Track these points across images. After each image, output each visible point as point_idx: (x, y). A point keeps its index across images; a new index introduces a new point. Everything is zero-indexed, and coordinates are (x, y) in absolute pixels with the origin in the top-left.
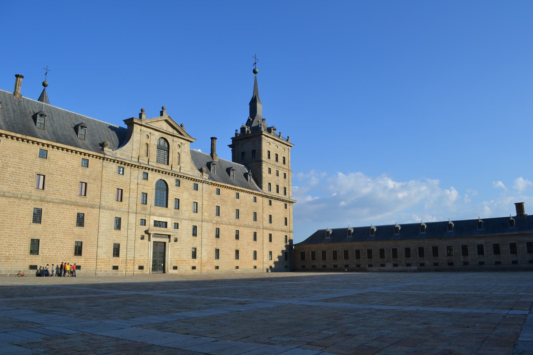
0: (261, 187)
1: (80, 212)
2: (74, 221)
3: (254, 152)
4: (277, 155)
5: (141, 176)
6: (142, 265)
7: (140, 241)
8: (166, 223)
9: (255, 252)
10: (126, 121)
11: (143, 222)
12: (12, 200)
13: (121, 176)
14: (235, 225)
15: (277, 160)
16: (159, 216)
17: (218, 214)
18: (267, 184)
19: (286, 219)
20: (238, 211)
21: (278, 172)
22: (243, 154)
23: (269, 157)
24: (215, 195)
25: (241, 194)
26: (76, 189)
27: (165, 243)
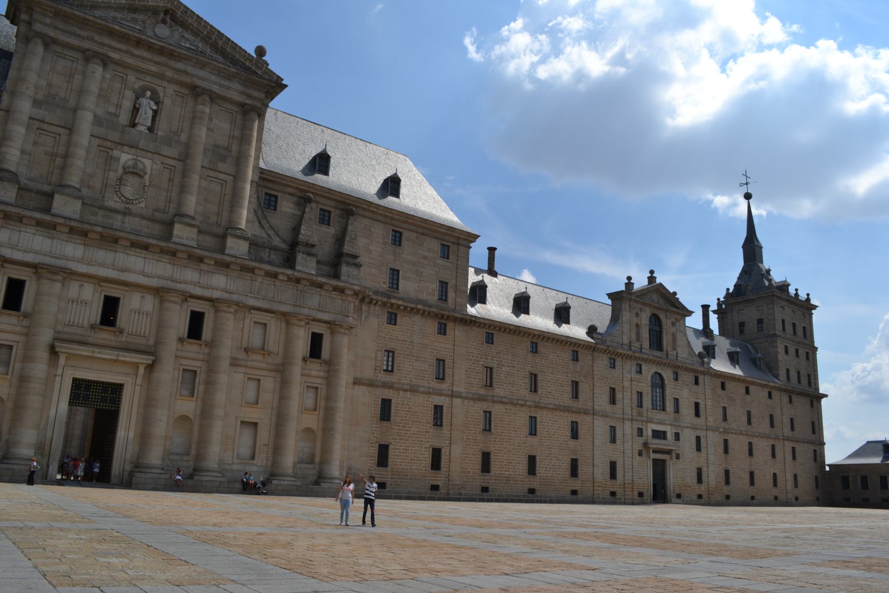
0: (777, 377)
1: (574, 420)
2: (568, 433)
3: (760, 321)
4: (794, 324)
5: (634, 368)
6: (641, 490)
7: (638, 458)
8: (664, 433)
9: (775, 475)
10: (610, 295)
11: (640, 432)
12: (508, 407)
13: (612, 370)
14: (747, 435)
15: (795, 333)
16: (658, 423)
17: (725, 419)
18: (785, 371)
19: (813, 423)
20: (749, 413)
21: (797, 351)
22: (742, 325)
23: (784, 329)
24: (719, 390)
25: (752, 388)
26: (568, 389)
27: (664, 461)
